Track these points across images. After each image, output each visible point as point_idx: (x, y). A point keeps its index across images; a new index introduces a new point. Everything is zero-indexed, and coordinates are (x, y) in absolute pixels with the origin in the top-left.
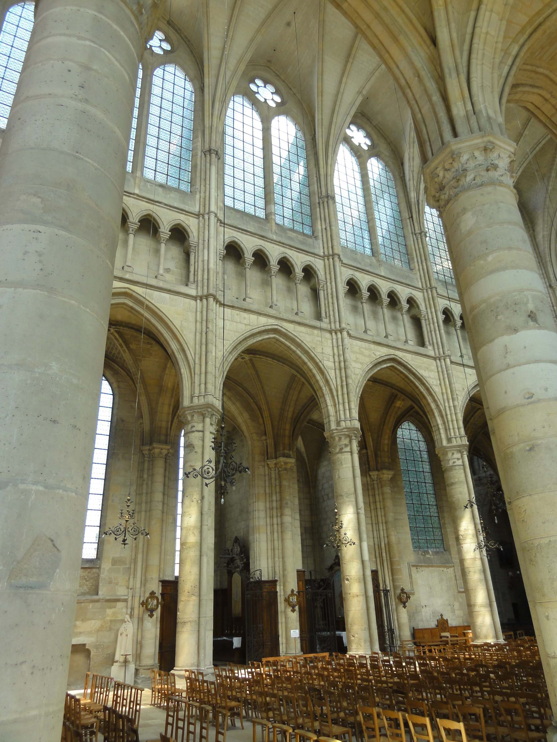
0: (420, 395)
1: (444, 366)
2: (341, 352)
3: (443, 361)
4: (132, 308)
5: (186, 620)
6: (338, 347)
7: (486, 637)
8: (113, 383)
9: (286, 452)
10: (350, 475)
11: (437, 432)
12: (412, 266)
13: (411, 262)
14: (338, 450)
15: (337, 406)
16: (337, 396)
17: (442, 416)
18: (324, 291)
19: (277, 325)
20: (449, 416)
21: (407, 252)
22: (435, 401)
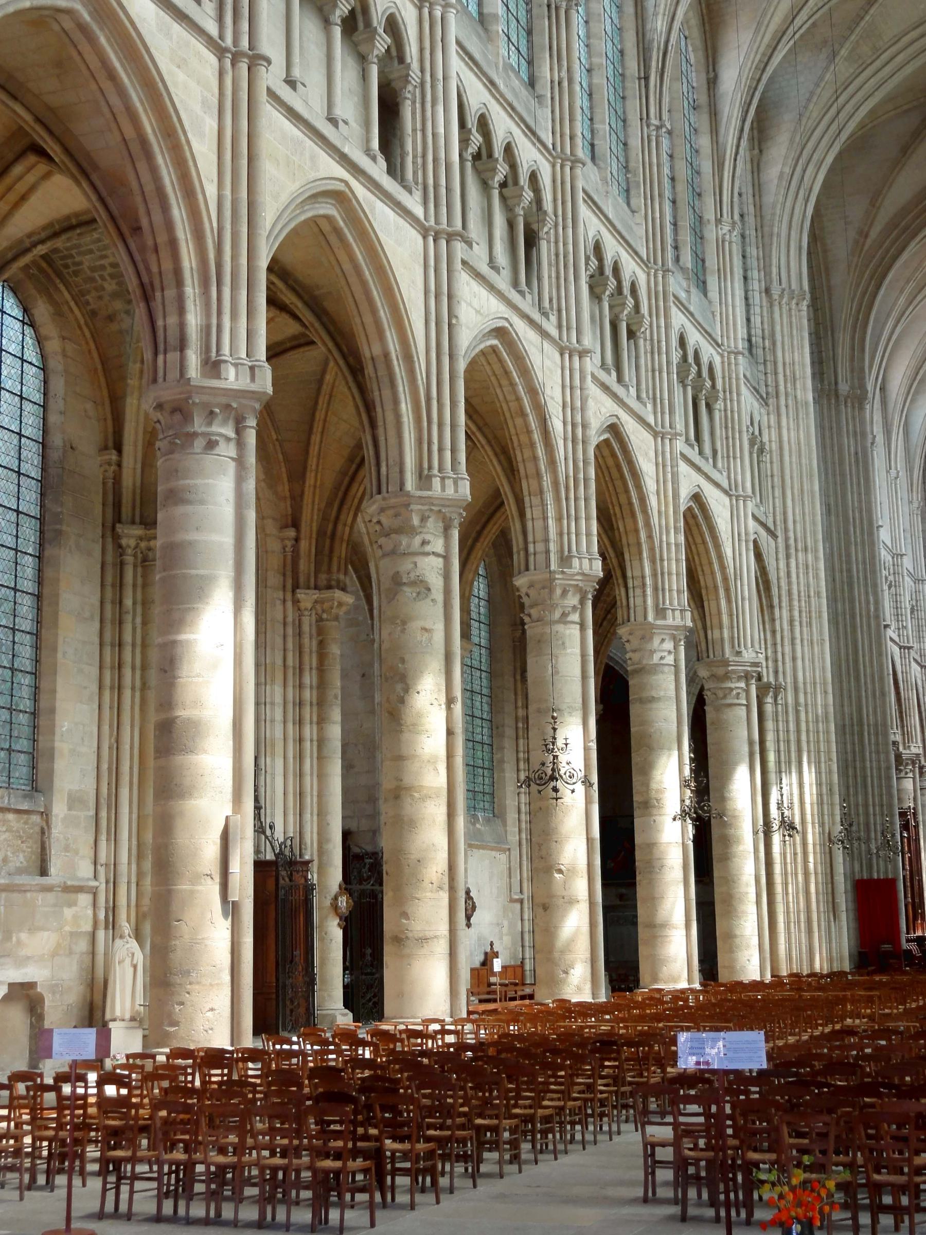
0: (625, 508)
1: (668, 455)
2: (578, 404)
3: (667, 441)
4: (337, 231)
5: (431, 934)
6: (571, 388)
7: (675, 980)
8: (47, 338)
9: (342, 577)
10: (577, 671)
11: (638, 592)
12: (633, 202)
13: (633, 192)
14: (557, 615)
15: (565, 522)
16: (567, 499)
17: (653, 561)
18: (549, 242)
19: (506, 319)
20: (666, 563)
21: (627, 162)
22: (648, 524)
